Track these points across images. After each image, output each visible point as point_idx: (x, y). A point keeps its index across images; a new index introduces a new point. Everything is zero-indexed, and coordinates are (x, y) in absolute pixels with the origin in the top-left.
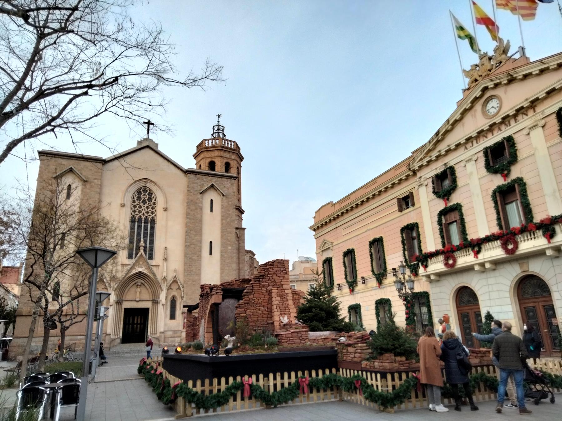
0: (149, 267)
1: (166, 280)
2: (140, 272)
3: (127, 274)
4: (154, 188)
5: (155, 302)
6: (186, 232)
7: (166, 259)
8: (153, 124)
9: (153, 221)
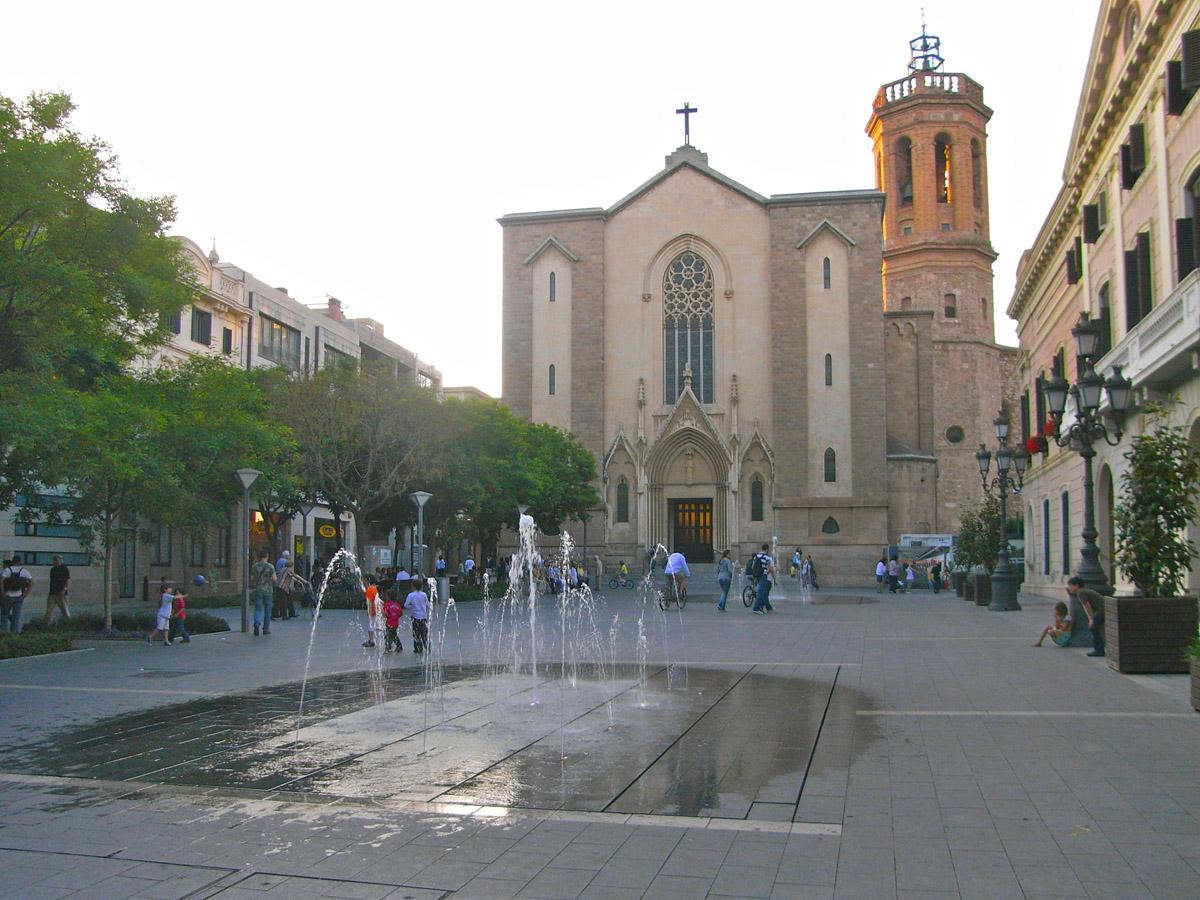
1: (739, 443)
2: (688, 429)
3: (663, 436)
4: (705, 253)
5: (722, 488)
6: (773, 339)
7: (735, 401)
8: (695, 110)
9: (709, 323)
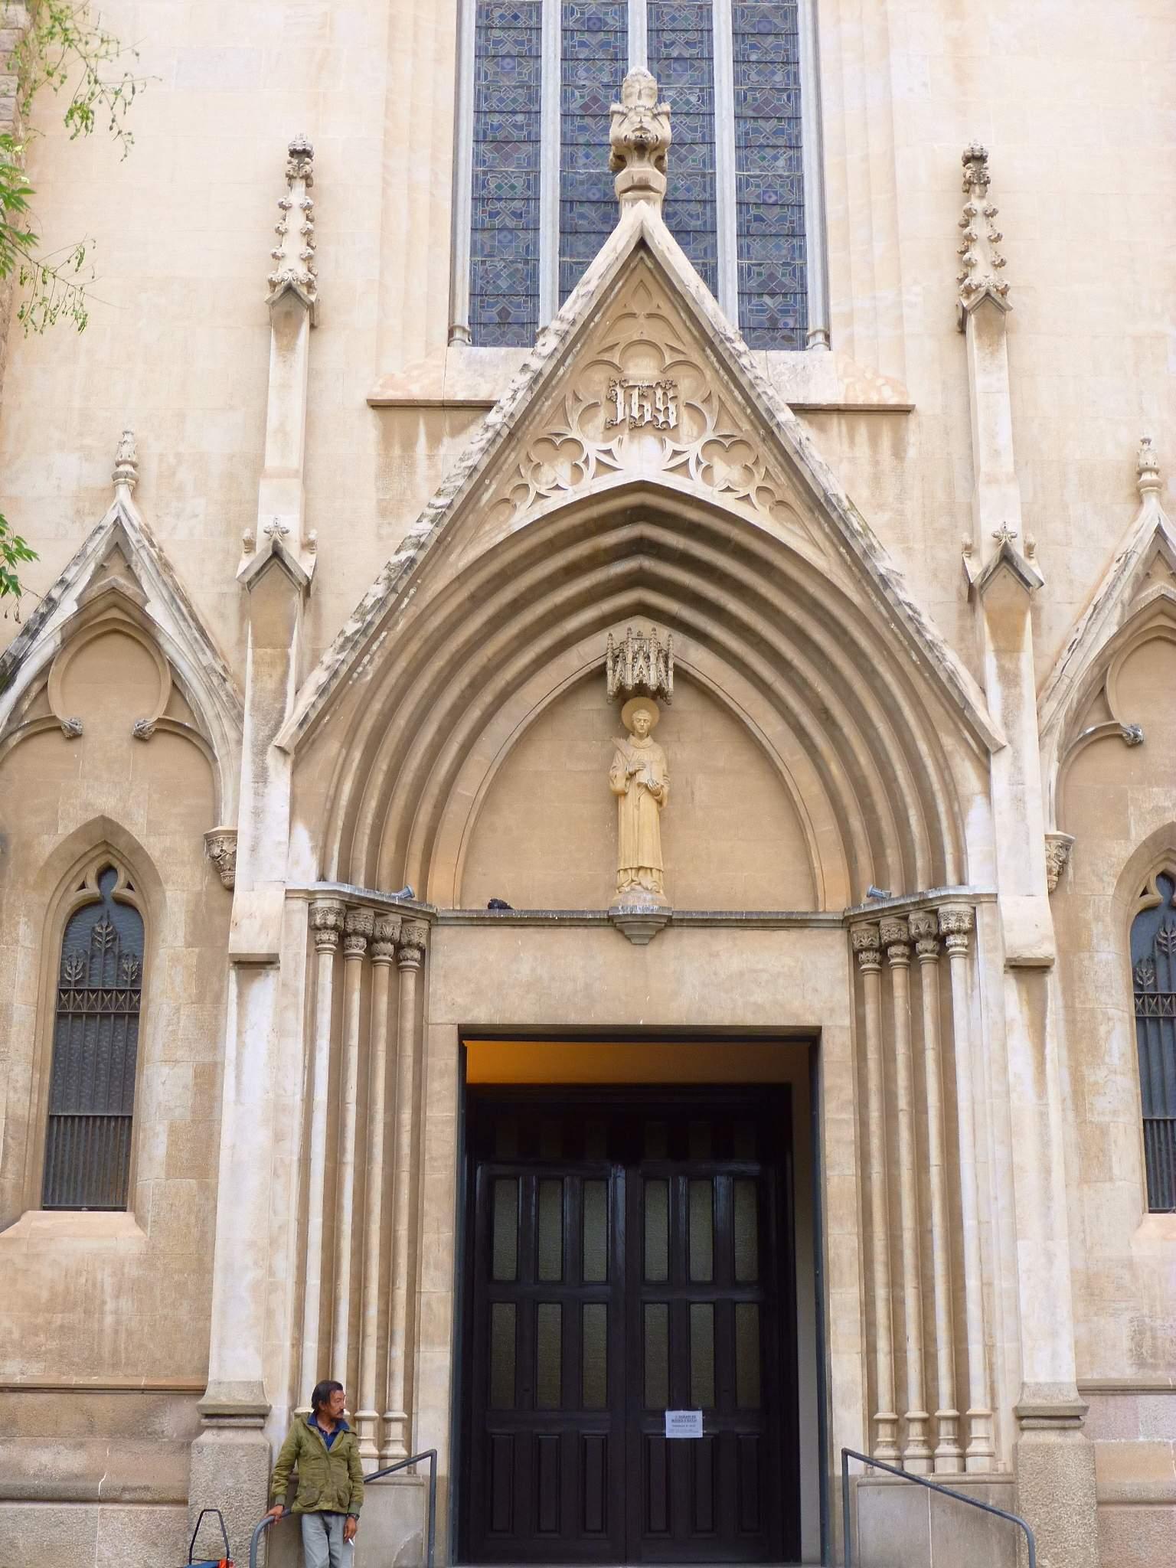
0: (758, 432)
2: (644, 507)
3: (454, 523)
7: (983, 311)
